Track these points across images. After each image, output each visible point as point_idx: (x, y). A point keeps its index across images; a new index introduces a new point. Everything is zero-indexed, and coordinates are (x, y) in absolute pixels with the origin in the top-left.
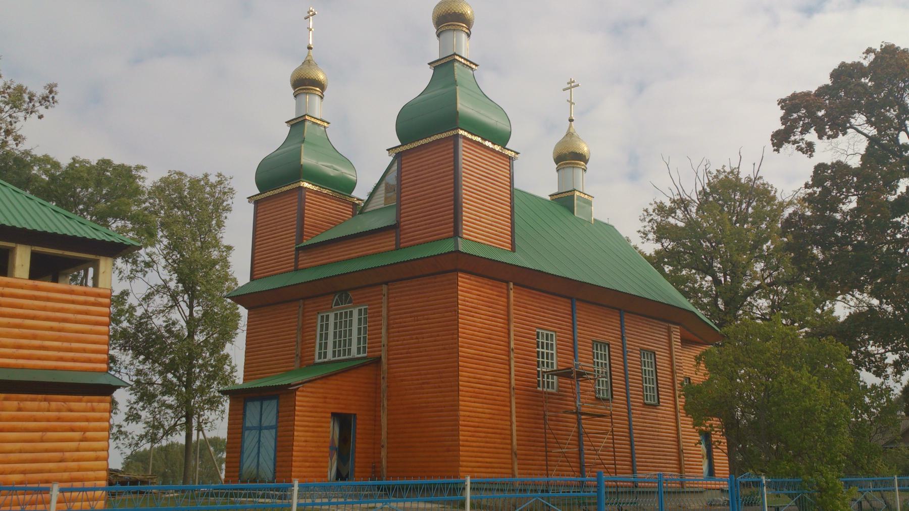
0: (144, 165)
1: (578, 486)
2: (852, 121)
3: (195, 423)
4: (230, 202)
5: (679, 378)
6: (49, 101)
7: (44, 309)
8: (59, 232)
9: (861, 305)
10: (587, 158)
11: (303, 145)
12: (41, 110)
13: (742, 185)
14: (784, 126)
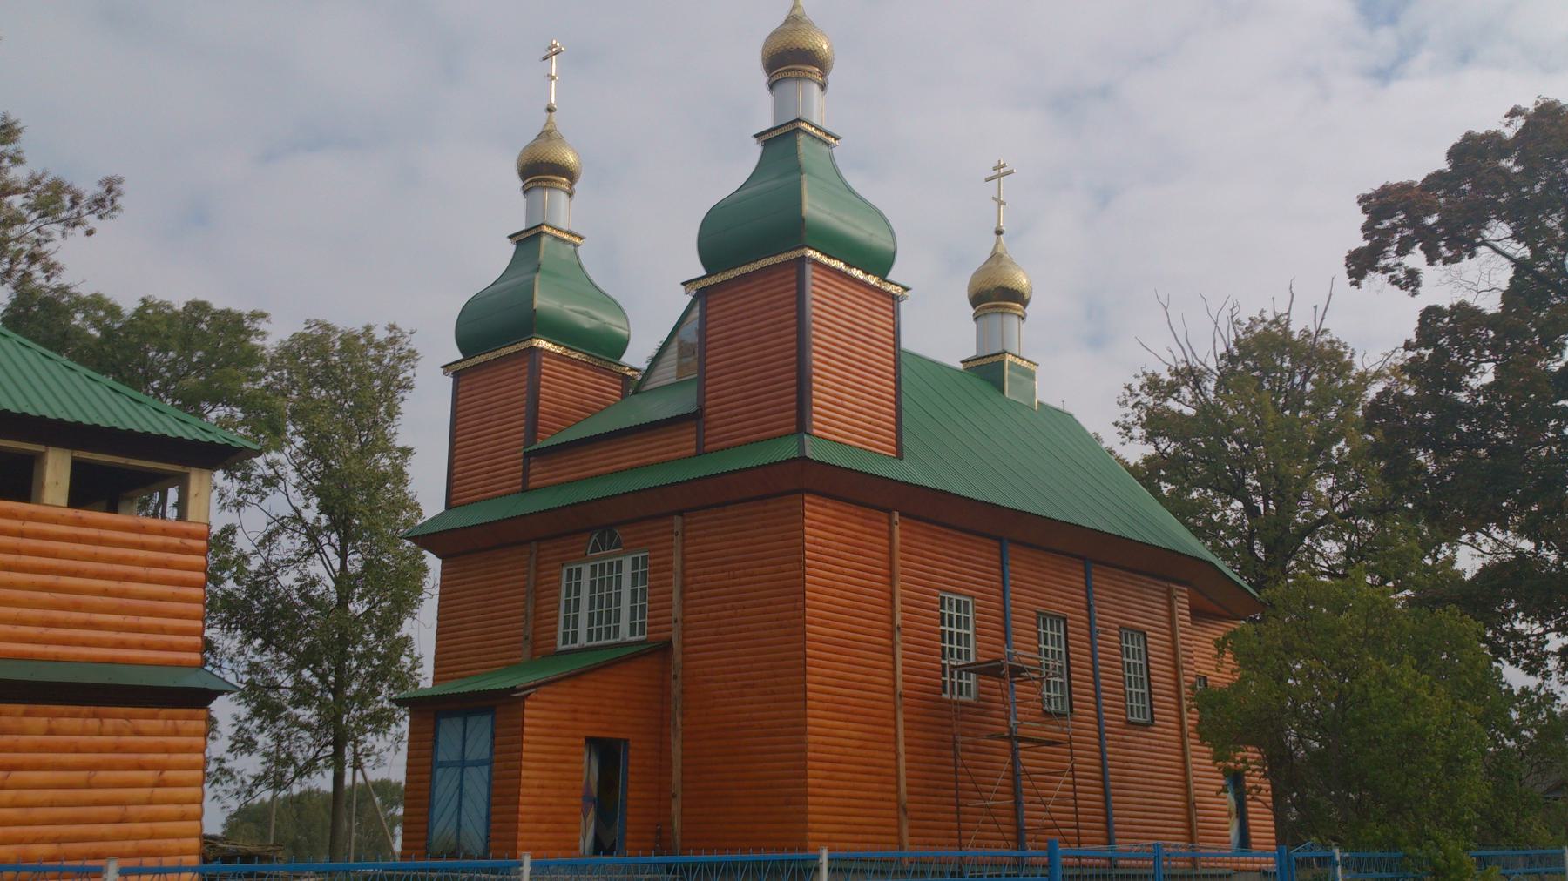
0: (265, 311)
1: (1014, 866)
2: (1486, 233)
4: (410, 373)
5: (1187, 679)
7: (94, 558)
8: (121, 427)
9: (1501, 551)
10: (1026, 297)
12: (92, 220)
13: (1295, 344)
14: (1368, 242)
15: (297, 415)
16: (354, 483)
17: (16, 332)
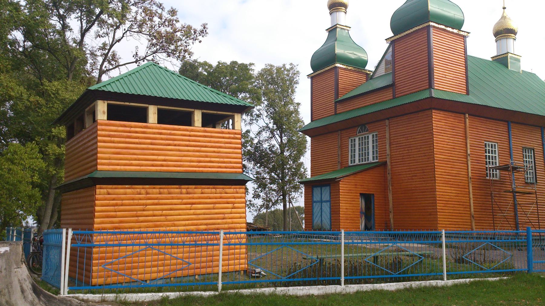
0: (253, 63)
3: (287, 199)
4: (297, 78)
6: (204, 33)
7: (210, 142)
11: (336, 42)
12: (200, 38)
15: (265, 94)
16: (283, 115)
17: (183, 75)
